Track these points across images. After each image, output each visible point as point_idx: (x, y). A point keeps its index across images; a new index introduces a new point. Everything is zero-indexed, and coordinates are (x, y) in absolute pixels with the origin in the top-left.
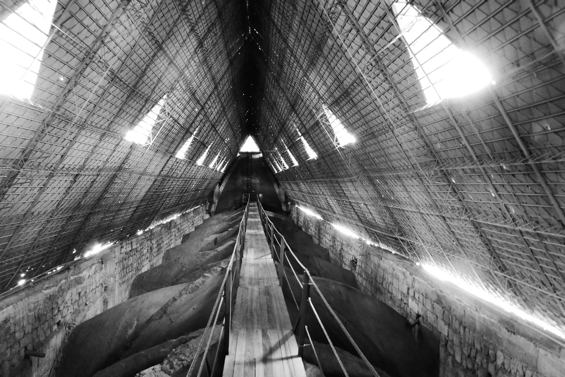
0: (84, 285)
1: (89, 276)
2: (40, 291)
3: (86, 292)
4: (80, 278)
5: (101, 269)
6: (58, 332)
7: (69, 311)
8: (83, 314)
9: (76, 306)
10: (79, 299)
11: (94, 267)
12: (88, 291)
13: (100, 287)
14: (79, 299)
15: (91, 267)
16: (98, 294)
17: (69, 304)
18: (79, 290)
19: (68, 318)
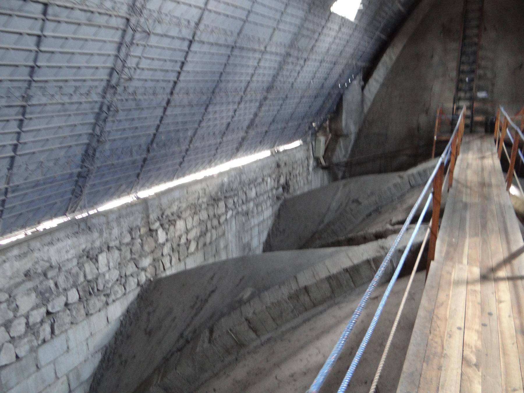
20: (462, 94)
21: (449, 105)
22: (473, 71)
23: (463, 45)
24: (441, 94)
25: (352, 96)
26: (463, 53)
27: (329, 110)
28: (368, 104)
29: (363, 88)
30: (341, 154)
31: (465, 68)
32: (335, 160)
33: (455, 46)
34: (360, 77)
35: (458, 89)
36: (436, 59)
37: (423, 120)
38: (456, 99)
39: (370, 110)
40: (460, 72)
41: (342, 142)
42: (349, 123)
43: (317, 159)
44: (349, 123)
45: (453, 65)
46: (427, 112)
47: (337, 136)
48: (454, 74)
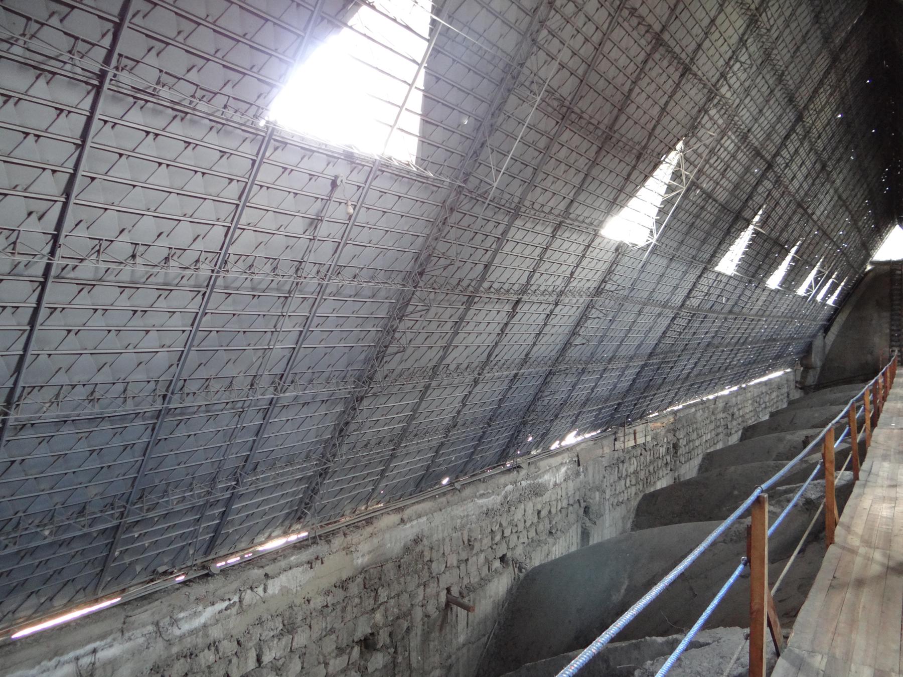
0: (546, 497)
1: (555, 485)
3: (550, 512)
4: (539, 485)
5: (578, 474)
7: (521, 540)
11: (563, 470)
12: (553, 511)
15: (557, 469)
16: (572, 517)
17: (521, 526)
18: (539, 507)
20: (894, 343)
21: (887, 349)
22: (899, 330)
23: (892, 315)
24: (880, 343)
25: (818, 342)
26: (892, 320)
27: (807, 350)
28: (828, 348)
29: (824, 337)
30: (811, 379)
31: (894, 328)
32: (807, 384)
33: (886, 314)
34: (822, 331)
35: (891, 341)
36: (874, 322)
37: (869, 357)
38: (891, 346)
39: (830, 350)
40: (891, 330)
41: (811, 372)
42: (816, 360)
43: (797, 382)
44: (816, 360)
45: (887, 325)
46: (871, 353)
47: (807, 368)
48: (888, 331)
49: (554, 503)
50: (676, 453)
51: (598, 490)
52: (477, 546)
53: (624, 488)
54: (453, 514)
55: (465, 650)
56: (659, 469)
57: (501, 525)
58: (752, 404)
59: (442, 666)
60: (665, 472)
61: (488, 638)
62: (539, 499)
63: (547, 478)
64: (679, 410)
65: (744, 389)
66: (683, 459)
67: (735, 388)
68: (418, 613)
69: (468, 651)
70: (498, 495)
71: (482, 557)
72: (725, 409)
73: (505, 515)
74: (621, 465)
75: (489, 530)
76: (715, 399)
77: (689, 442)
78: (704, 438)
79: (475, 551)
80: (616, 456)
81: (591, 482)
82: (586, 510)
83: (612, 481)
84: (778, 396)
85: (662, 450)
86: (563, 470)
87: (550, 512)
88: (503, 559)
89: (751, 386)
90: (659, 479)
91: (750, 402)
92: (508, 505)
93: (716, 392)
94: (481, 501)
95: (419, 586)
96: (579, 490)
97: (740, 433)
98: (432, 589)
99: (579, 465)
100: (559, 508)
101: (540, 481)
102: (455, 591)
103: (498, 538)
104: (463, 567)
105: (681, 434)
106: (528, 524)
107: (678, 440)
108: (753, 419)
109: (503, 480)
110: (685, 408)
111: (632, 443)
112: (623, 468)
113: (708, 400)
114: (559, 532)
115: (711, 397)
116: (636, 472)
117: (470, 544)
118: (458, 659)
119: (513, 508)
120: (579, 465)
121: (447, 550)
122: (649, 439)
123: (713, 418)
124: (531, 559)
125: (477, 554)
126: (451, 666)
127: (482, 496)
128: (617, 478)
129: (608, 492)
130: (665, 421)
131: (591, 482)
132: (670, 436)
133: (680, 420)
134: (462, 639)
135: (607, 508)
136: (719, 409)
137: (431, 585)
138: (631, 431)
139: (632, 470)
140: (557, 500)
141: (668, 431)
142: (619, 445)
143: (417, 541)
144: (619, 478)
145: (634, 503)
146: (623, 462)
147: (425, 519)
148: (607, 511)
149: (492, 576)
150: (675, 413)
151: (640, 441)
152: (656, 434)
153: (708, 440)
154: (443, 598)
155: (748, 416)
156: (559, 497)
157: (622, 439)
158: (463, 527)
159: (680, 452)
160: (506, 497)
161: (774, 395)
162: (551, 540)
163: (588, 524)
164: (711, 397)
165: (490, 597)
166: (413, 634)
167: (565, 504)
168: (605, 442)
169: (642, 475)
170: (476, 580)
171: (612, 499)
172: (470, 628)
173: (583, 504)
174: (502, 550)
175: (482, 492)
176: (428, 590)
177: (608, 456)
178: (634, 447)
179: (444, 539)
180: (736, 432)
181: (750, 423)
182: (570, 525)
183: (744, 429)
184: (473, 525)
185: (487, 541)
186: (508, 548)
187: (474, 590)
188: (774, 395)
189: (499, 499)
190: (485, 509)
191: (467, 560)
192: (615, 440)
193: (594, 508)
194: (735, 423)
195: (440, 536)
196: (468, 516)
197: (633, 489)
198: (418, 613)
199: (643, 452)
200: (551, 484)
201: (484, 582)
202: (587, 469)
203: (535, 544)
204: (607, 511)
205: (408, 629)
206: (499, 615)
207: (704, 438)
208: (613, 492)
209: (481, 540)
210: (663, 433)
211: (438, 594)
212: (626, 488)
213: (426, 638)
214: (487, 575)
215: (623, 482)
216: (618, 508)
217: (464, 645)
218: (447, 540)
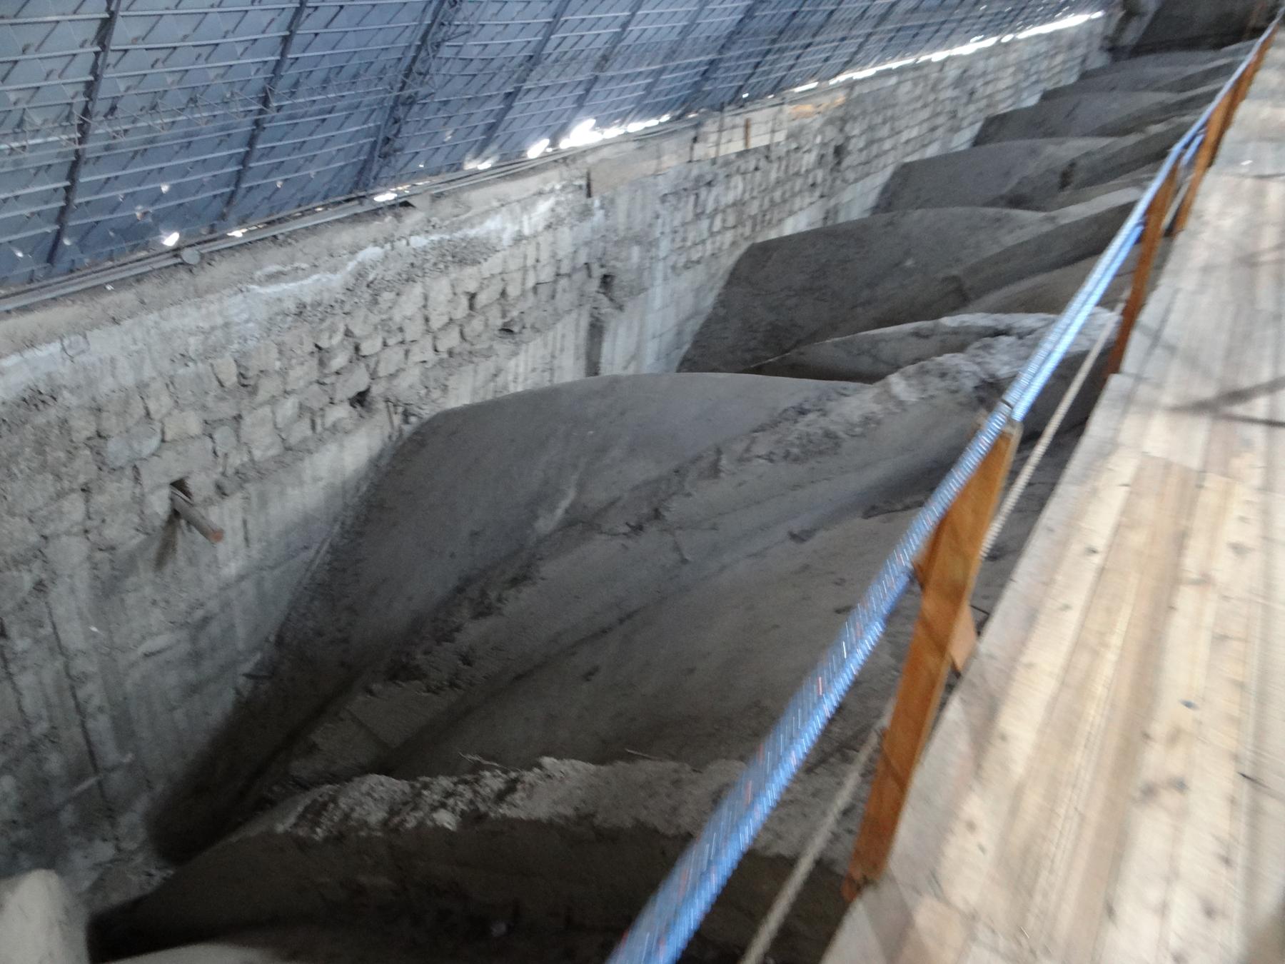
0: (491, 265)
1: (519, 239)
2: (238, 285)
3: (503, 294)
4: (470, 242)
5: (586, 213)
6: (347, 433)
7: (416, 356)
8: (486, 367)
9: (451, 340)
10: (470, 317)
11: (543, 207)
12: (513, 291)
13: (580, 276)
14: (470, 317)
15: (526, 205)
16: (565, 299)
17: (414, 330)
18: (472, 287)
19: (408, 383)
49: (518, 276)
50: (839, 163)
51: (639, 243)
52: (268, 387)
53: (706, 234)
54: (167, 326)
55: (247, 585)
56: (794, 195)
57: (348, 333)
58: (1014, 74)
59: (175, 625)
60: (808, 200)
61: (318, 552)
62: (470, 270)
63: (497, 226)
64: (863, 81)
65: (1007, 44)
66: (851, 175)
67: (991, 41)
68: (72, 553)
69: (259, 584)
70: (334, 270)
71: (289, 407)
72: (959, 82)
73: (362, 313)
74: (703, 192)
75: (309, 347)
76: (943, 64)
77: (870, 143)
78: (905, 136)
79: (262, 395)
80: (695, 172)
81: (621, 228)
82: (606, 281)
83: (677, 223)
84: (1064, 62)
85: (810, 159)
86: (543, 207)
87: (503, 294)
88: (361, 400)
89: (1020, 41)
90: (791, 213)
91: (1011, 70)
92: (368, 288)
93: (950, 47)
94: (272, 290)
95: (60, 495)
96: (587, 244)
97: (978, 126)
98: (117, 491)
99: (589, 195)
100: (530, 283)
101: (472, 233)
102: (200, 484)
103: (339, 361)
104: (222, 434)
105: (855, 129)
106: (436, 323)
107: (848, 139)
108: (1010, 101)
109: (346, 236)
110: (880, 75)
111: (738, 146)
112: (709, 199)
113: (928, 63)
114: (527, 332)
115: (938, 56)
116: (739, 204)
117: (246, 384)
118: (226, 605)
119: (387, 296)
120: (589, 195)
121: (160, 404)
122: (780, 137)
123: (931, 98)
124: (445, 388)
125: (273, 401)
126: (206, 620)
127: (274, 278)
128: (690, 216)
129: (665, 246)
130: (825, 101)
131: (621, 228)
132: (831, 133)
133: (860, 100)
134: (232, 569)
135: (659, 275)
136: (948, 81)
137: (112, 486)
138: (740, 121)
139: (730, 197)
140: (524, 269)
141: (830, 122)
142: (700, 150)
143: (34, 400)
144: (698, 216)
145: (728, 262)
146: (709, 184)
147: (55, 348)
148: (659, 281)
149: (321, 440)
150: (851, 85)
151: (758, 141)
152: (802, 128)
153: (914, 139)
154: (159, 505)
155: (999, 97)
156: (530, 262)
157: (713, 138)
158: (210, 353)
159: (847, 161)
160: (360, 274)
161: (1059, 59)
162: (503, 347)
163: (606, 307)
164: (938, 56)
165: (316, 480)
166: (58, 592)
167: (546, 274)
168: (669, 145)
169: (754, 208)
170: (273, 452)
171: (673, 258)
172: (256, 547)
173: (598, 272)
174: (359, 380)
175: (273, 268)
176: (100, 500)
177: (672, 173)
178: (740, 155)
179: (142, 387)
180: (972, 124)
181: (1002, 108)
182: (558, 316)
183: (987, 119)
184: (252, 343)
185: (302, 373)
186: (374, 376)
187: (262, 474)
188: (1059, 59)
189: (337, 281)
190: (290, 305)
191: (238, 418)
192: (695, 140)
193: (623, 280)
194: (972, 108)
195: (129, 380)
196: (227, 325)
197: (729, 236)
198: (72, 553)
199: (763, 163)
200: (507, 238)
201: (291, 453)
202: (612, 201)
203: (454, 361)
204: (659, 281)
205: (40, 587)
206: (346, 506)
207: (905, 136)
208: (678, 244)
209: (283, 373)
210: (817, 125)
211: (140, 501)
212: (712, 234)
213: (109, 588)
214: (304, 440)
215: (705, 224)
216: (688, 275)
217: (241, 578)
218: (157, 385)
